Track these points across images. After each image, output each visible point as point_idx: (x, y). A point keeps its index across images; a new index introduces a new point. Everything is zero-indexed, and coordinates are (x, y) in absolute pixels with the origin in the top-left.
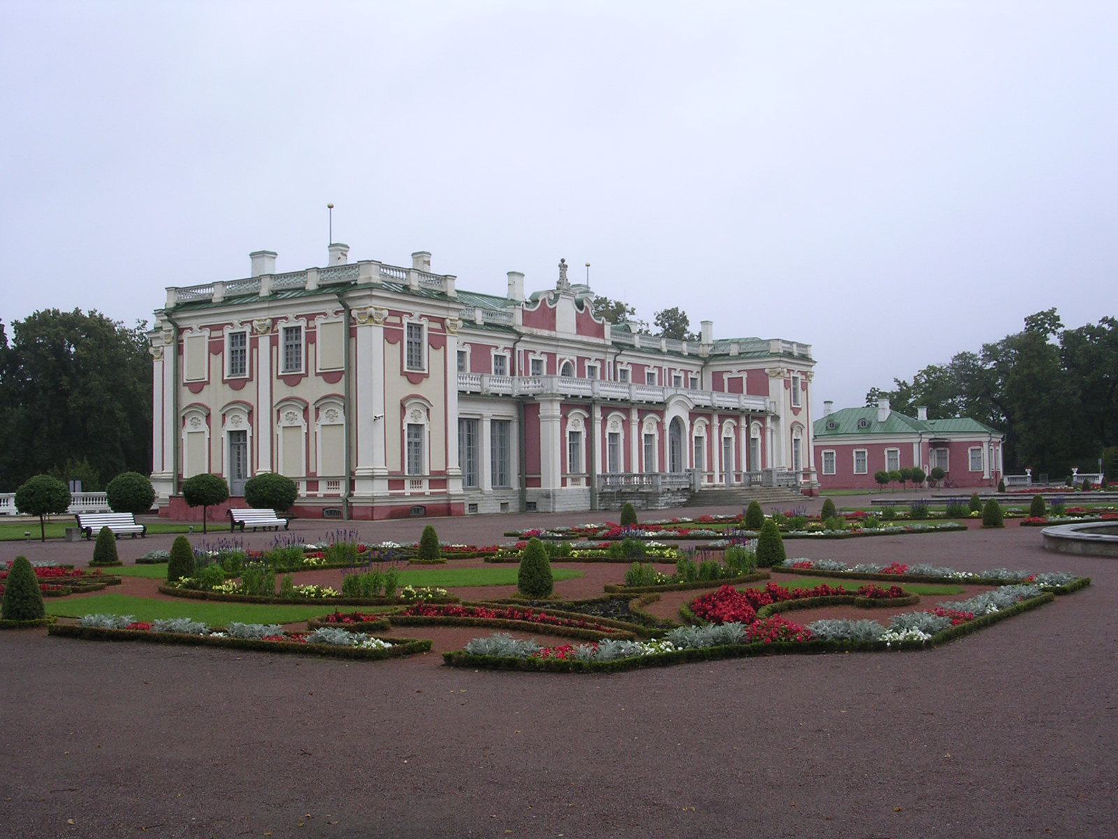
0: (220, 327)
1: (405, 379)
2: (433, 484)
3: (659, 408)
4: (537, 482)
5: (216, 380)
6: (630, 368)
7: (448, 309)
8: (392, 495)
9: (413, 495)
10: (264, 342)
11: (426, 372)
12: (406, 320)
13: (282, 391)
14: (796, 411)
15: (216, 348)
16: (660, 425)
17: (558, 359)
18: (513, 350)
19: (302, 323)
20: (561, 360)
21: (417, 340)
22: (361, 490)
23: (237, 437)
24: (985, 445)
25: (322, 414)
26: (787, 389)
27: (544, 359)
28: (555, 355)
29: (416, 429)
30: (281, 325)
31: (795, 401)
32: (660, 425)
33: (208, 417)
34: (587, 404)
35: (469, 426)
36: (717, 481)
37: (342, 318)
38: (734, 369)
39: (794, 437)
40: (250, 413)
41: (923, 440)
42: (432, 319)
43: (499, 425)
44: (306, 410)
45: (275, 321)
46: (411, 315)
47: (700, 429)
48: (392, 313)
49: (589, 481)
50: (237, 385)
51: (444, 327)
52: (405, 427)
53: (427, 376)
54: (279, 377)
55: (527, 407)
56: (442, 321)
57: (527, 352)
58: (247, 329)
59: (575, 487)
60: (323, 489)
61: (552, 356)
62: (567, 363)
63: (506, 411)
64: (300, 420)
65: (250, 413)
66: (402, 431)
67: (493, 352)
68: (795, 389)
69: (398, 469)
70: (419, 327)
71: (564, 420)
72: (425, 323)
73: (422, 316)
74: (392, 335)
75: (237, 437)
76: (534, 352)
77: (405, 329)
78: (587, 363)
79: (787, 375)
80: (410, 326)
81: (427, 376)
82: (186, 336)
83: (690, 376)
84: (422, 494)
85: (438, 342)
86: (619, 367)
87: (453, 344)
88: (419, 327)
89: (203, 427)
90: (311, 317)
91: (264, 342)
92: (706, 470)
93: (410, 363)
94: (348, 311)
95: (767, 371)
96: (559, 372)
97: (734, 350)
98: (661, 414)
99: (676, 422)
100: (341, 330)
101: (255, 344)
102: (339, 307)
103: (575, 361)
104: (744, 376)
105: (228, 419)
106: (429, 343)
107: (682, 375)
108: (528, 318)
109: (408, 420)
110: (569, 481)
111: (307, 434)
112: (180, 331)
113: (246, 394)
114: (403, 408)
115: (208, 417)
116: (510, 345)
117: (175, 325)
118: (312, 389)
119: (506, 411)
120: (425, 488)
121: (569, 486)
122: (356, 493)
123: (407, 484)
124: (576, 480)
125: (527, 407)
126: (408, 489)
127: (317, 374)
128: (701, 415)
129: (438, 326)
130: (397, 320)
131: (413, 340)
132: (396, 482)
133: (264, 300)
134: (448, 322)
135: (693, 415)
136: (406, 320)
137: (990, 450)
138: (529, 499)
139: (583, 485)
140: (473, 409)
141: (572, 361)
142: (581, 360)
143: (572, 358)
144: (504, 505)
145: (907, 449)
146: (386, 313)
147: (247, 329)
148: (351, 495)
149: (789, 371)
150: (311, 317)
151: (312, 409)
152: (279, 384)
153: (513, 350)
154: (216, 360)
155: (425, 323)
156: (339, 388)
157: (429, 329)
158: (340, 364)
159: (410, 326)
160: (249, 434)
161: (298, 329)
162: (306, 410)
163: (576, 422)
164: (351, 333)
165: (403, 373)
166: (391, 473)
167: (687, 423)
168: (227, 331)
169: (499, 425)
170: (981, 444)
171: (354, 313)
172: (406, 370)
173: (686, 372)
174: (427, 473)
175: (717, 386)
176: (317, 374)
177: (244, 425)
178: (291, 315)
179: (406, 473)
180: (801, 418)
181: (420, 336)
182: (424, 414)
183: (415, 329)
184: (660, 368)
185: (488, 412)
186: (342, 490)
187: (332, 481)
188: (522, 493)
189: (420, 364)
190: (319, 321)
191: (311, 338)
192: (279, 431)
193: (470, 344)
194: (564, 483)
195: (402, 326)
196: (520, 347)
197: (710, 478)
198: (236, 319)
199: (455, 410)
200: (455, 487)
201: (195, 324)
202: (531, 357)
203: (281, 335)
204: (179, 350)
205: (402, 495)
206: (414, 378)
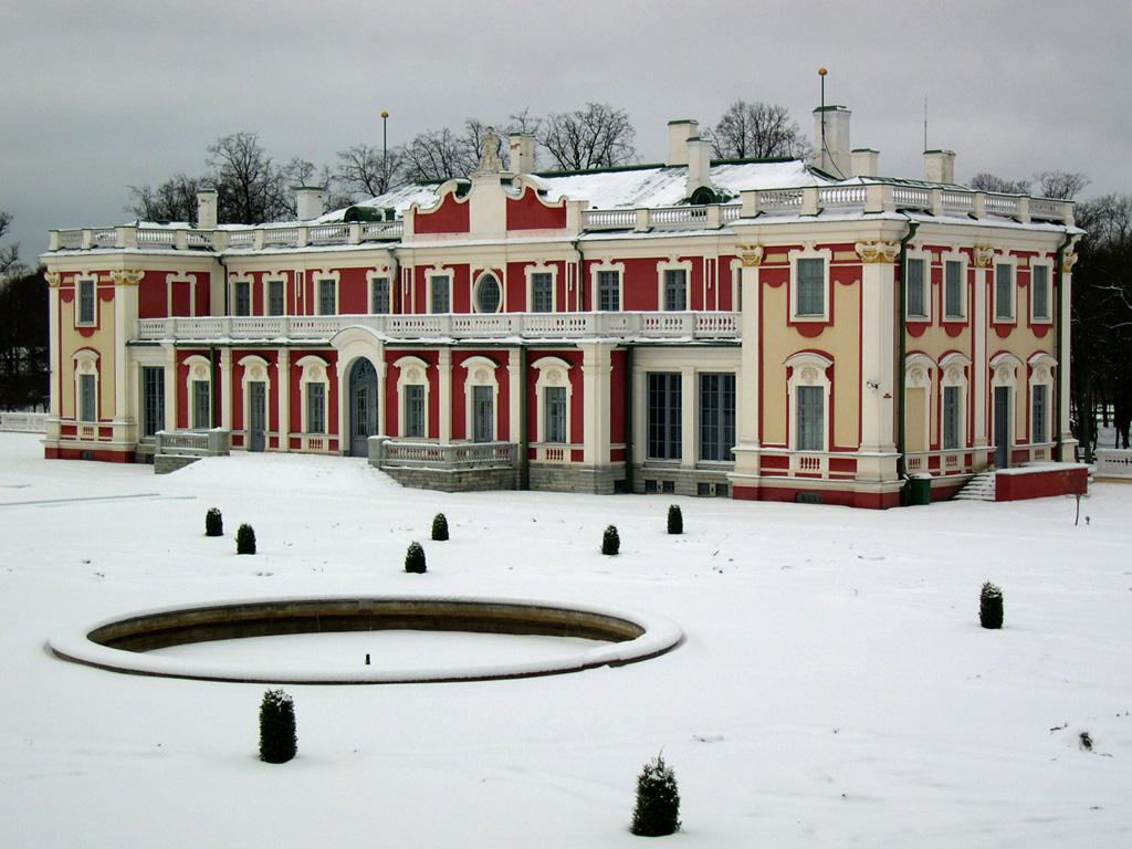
6: (620, 268)
16: (331, 371)
17: (472, 271)
20: (477, 273)
26: (775, 284)
27: (450, 273)
28: (468, 266)
32: (331, 371)
34: (213, 353)
47: (412, 372)
57: (420, 270)
76: (433, 267)
77: (77, 288)
78: (529, 271)
86: (594, 269)
99: (362, 367)
103: (504, 271)
135: (391, 356)
141: (499, 272)
142: (516, 269)
143: (495, 267)
163: (199, 369)
165: (76, 329)
167: (380, 367)
189: (92, 319)
193: (339, 270)
195: (73, 284)
196: (407, 264)
206: (87, 332)
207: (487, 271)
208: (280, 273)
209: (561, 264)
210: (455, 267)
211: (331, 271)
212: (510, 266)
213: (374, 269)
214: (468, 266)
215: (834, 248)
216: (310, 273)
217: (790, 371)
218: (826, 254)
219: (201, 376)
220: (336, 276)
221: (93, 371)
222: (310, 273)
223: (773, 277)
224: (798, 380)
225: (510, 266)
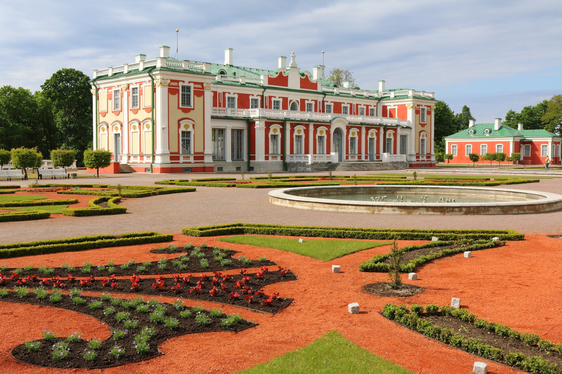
0: (110, 88)
1: (180, 111)
2: (195, 158)
3: (328, 125)
4: (254, 158)
5: (110, 111)
6: (332, 104)
7: (205, 78)
8: (171, 163)
9: (184, 163)
10: (125, 94)
11: (192, 107)
12: (181, 84)
13: (132, 116)
14: (423, 125)
15: (109, 97)
16: (328, 133)
18: (262, 96)
19: (138, 86)
20: (291, 101)
21: (188, 93)
22: (158, 160)
23: (117, 136)
24: (550, 144)
25: (145, 126)
27: (281, 100)
28: (287, 98)
29: (186, 134)
30: (131, 87)
31: (423, 120)
32: (328, 133)
33: (108, 127)
34: (283, 123)
35: (219, 132)
36: (363, 158)
37: (151, 84)
38: (392, 104)
39: (421, 138)
40: (122, 126)
41: (515, 140)
42: (195, 83)
43: (237, 133)
44: (140, 124)
45: (129, 85)
46: (184, 82)
48: (172, 81)
49: (283, 158)
50: (117, 113)
51: (203, 89)
52: (180, 133)
53: (193, 109)
54: (131, 110)
55: (250, 123)
56: (202, 84)
57: (270, 97)
58: (120, 89)
59: (274, 160)
60: (145, 160)
61: (285, 99)
62: (293, 103)
63: (242, 125)
64: (137, 130)
65: (122, 126)
66: (179, 135)
67: (251, 97)
68: (423, 114)
69: (177, 151)
70: (189, 88)
71: (267, 130)
72: (192, 85)
73: (189, 82)
74: (172, 91)
75: (117, 136)
76: (275, 97)
78: (306, 102)
79: (418, 107)
80: (183, 87)
81: (193, 109)
82: (100, 91)
83: (370, 108)
84: (190, 163)
85: (200, 93)
86: (326, 104)
87: (209, 96)
88: (189, 88)
89: (106, 132)
90: (141, 83)
91: (125, 94)
92: (357, 152)
93: (182, 104)
94: (153, 80)
95: (406, 106)
96: (289, 107)
97: (392, 95)
98: (329, 127)
99: (338, 131)
100: (150, 89)
101: (122, 94)
102: (150, 78)
103: (299, 101)
104: (396, 107)
105: (114, 128)
106: (194, 94)
107: (365, 107)
108: (271, 81)
109: (182, 129)
110: (270, 158)
111: (140, 135)
112: (97, 90)
113: (119, 118)
114: (179, 126)
115: (108, 127)
116: (261, 94)
117: (96, 87)
118: (142, 115)
119: (242, 125)
120: (192, 160)
121: (270, 159)
122: (156, 162)
123: (181, 158)
124: (274, 157)
125: (250, 123)
126: (182, 160)
127: (143, 109)
128: (352, 127)
129: (200, 86)
130: (176, 84)
131: (186, 93)
132: (174, 157)
133: (125, 75)
134: (205, 85)
135: (348, 128)
136: (181, 84)
137: (553, 147)
138: (251, 165)
139: (279, 159)
140: (220, 124)
142: (303, 101)
144: (238, 169)
145: (507, 144)
146: (169, 81)
147: (120, 89)
148: (153, 162)
149: (418, 105)
150: (141, 83)
151: (142, 124)
152: (130, 112)
153: (262, 96)
154: (110, 101)
155: (192, 85)
156: (150, 115)
157: (194, 88)
158: (149, 104)
159: (183, 87)
160: (121, 135)
161: (137, 88)
162: (140, 124)
163: (275, 129)
164: (154, 90)
165: (179, 108)
166: (171, 153)
167: (345, 131)
168: (114, 89)
169: (237, 133)
170: (547, 143)
171: (155, 81)
172: (181, 106)
173: (367, 106)
174: (192, 152)
175: (384, 114)
176: (143, 109)
177: (119, 132)
178: (134, 82)
179: (181, 152)
180: (426, 128)
181: (189, 91)
182: (191, 127)
183: (186, 89)
184: (351, 104)
185: (229, 126)
186: (151, 161)
187: (135, 156)
188: (249, 163)
189: (189, 104)
190: (144, 84)
191: (141, 94)
192: (131, 134)
193: (238, 94)
194: (267, 158)
195: (178, 86)
197: (360, 157)
198: (116, 84)
199: (210, 125)
200: (208, 160)
201: (101, 86)
202: (273, 99)
203: (131, 91)
204: (97, 98)
205: (179, 163)
207: (294, 101)
208: (234, 94)
209: (316, 101)
210: (283, 98)
211: (234, 94)
212: (301, 99)
213: (253, 95)
214: (287, 98)
215: (428, 106)
216: (224, 93)
217: (420, 135)
218: (426, 108)
219: (275, 133)
220: (236, 96)
221: (190, 129)
222: (224, 93)
223: (417, 112)
224: (421, 138)
225: (301, 99)
